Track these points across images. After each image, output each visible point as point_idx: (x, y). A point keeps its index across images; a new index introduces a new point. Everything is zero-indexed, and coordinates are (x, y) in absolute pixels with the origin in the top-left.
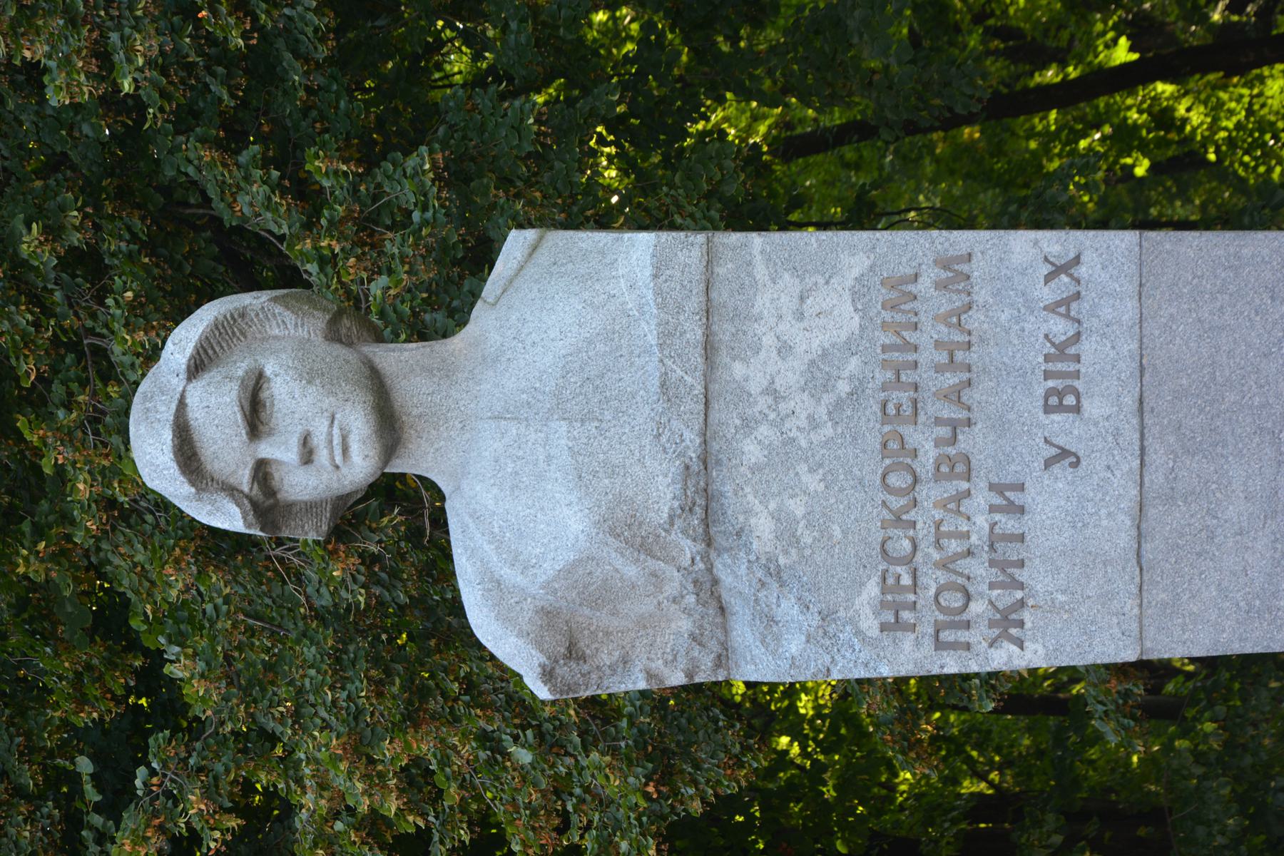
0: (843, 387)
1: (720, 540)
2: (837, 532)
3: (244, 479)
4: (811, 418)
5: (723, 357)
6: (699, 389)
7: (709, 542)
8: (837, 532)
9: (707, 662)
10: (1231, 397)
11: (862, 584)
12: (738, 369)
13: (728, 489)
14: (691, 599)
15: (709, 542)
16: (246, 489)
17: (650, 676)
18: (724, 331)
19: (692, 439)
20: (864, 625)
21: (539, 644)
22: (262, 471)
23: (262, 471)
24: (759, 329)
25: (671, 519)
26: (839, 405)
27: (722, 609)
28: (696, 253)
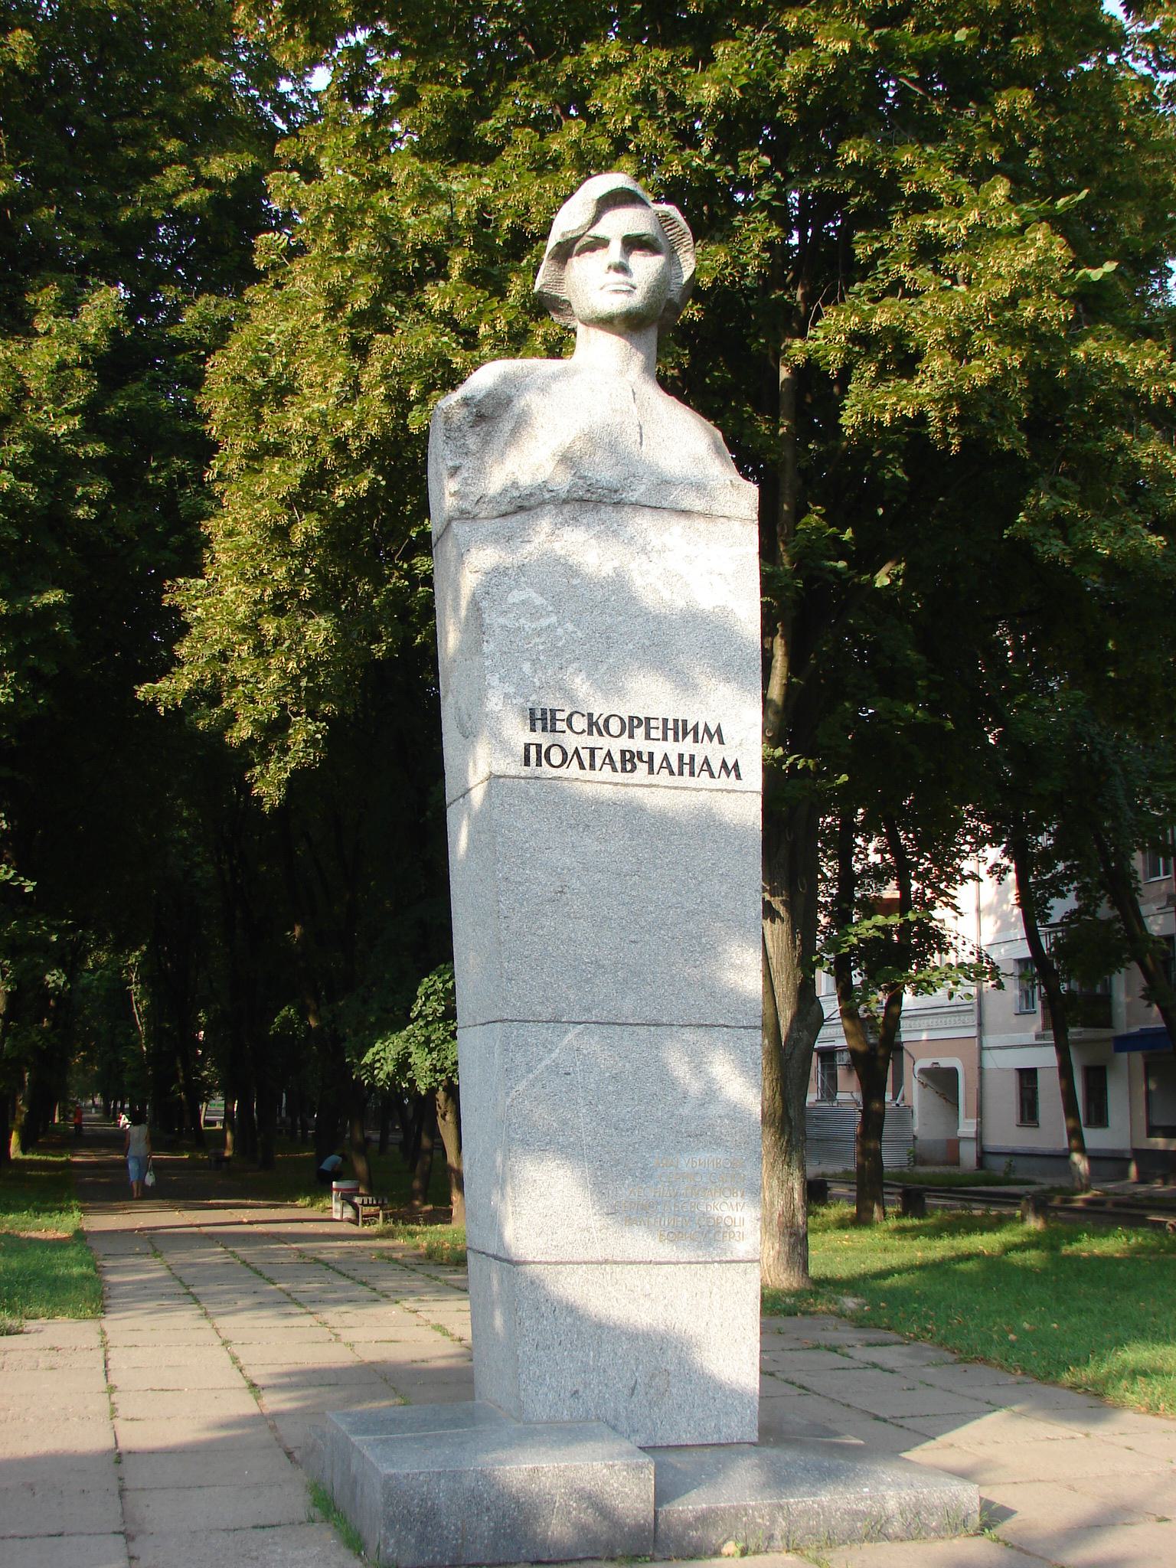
1: (567, 508)
3: (599, 231)
4: (648, 572)
6: (665, 504)
7: (565, 502)
10: (660, 844)
11: (542, 595)
13: (603, 516)
14: (516, 494)
15: (565, 502)
16: (591, 232)
19: (633, 497)
20: (515, 592)
21: (488, 395)
22: (600, 243)
23: (600, 243)
25: (584, 477)
27: (504, 515)
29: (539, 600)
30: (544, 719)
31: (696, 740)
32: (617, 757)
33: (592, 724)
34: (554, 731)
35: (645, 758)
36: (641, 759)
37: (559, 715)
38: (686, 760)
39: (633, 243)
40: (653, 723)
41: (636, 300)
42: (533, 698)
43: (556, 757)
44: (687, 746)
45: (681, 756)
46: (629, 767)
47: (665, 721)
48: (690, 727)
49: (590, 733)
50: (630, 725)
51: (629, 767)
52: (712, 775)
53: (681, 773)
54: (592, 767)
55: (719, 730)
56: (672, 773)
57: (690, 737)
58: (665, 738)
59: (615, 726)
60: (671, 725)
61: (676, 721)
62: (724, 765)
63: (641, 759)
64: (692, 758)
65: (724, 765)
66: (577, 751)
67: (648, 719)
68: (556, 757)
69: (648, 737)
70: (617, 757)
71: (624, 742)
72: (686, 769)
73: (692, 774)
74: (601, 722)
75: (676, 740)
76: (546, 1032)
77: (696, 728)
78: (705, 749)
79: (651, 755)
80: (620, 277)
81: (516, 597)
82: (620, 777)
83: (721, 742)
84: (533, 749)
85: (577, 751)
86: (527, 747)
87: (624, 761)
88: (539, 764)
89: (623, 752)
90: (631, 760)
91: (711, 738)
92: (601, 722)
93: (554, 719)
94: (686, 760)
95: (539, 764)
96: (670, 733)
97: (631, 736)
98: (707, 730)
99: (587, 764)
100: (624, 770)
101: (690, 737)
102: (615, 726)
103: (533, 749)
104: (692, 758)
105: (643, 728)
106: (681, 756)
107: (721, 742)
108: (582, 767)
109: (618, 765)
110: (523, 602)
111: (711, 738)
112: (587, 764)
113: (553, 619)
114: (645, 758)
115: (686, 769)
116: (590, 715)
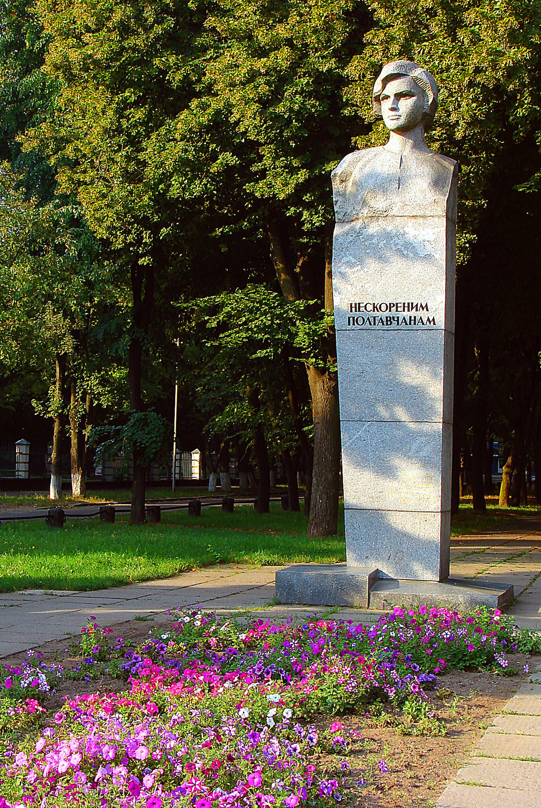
0: (405, 252)
2: (368, 251)
3: (386, 92)
5: (413, 220)
8: (368, 251)
9: (340, 217)
12: (410, 225)
17: (337, 202)
18: (421, 220)
22: (387, 97)
23: (387, 97)
24: (421, 230)
26: (401, 251)
28: (441, 213)
29: (353, 260)
30: (356, 307)
31: (417, 310)
32: (384, 320)
33: (374, 307)
34: (359, 311)
35: (396, 319)
36: (394, 320)
37: (361, 305)
38: (413, 318)
39: (399, 96)
40: (399, 305)
41: (402, 121)
42: (352, 299)
43: (360, 321)
44: (413, 313)
45: (410, 317)
46: (389, 323)
47: (404, 304)
48: (414, 305)
49: (374, 311)
50: (389, 307)
51: (389, 323)
52: (423, 324)
53: (410, 324)
54: (375, 324)
55: (426, 305)
56: (406, 324)
57: (414, 309)
58: (404, 311)
59: (383, 308)
60: (406, 305)
61: (409, 304)
62: (428, 319)
63: (394, 320)
64: (415, 317)
65: (428, 319)
66: (368, 319)
67: (397, 304)
68: (360, 321)
69: (397, 311)
70: (384, 320)
71: (387, 313)
72: (412, 322)
73: (415, 324)
74: (378, 307)
75: (409, 311)
76: (356, 425)
77: (417, 305)
78: (423, 314)
79: (398, 317)
80: (393, 113)
81: (345, 260)
82: (385, 327)
83: (427, 310)
84: (351, 319)
85: (368, 319)
86: (349, 318)
87: (387, 321)
88: (354, 324)
89: (387, 318)
90: (390, 320)
91: (423, 309)
92: (378, 307)
93: (359, 307)
94: (413, 318)
95: (354, 324)
96: (406, 309)
97: (390, 311)
98: (421, 306)
99: (372, 324)
100: (387, 324)
101: (414, 309)
102: (383, 308)
103: (351, 319)
104: (415, 317)
105: (395, 307)
106: (410, 317)
107: (427, 310)
108: (370, 324)
109: (385, 323)
110: (347, 262)
111: (423, 309)
112: (372, 324)
113: (359, 267)
114: (396, 319)
115: (412, 322)
116: (374, 304)
